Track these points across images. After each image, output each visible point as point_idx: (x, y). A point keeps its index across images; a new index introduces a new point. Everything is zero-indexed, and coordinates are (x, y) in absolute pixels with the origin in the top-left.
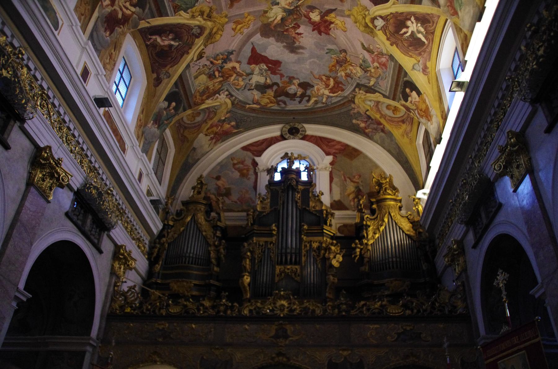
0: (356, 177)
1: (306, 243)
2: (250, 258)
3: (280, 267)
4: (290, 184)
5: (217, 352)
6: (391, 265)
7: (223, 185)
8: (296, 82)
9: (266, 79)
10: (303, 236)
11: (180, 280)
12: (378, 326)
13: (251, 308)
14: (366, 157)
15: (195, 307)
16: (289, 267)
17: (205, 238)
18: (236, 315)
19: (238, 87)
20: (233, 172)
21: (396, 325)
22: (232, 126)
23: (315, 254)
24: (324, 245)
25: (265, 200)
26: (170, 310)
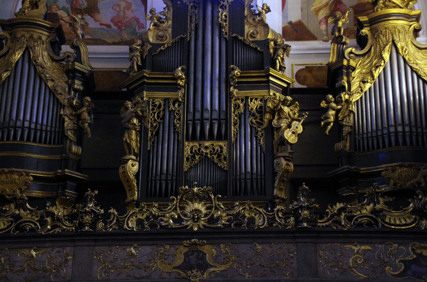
3: (191, 144)
6: (393, 139)
10: (232, 88)
15: (36, 219)
17: (52, 92)
18: (114, 229)
23: (254, 121)
24: (270, 104)
25: (163, 22)
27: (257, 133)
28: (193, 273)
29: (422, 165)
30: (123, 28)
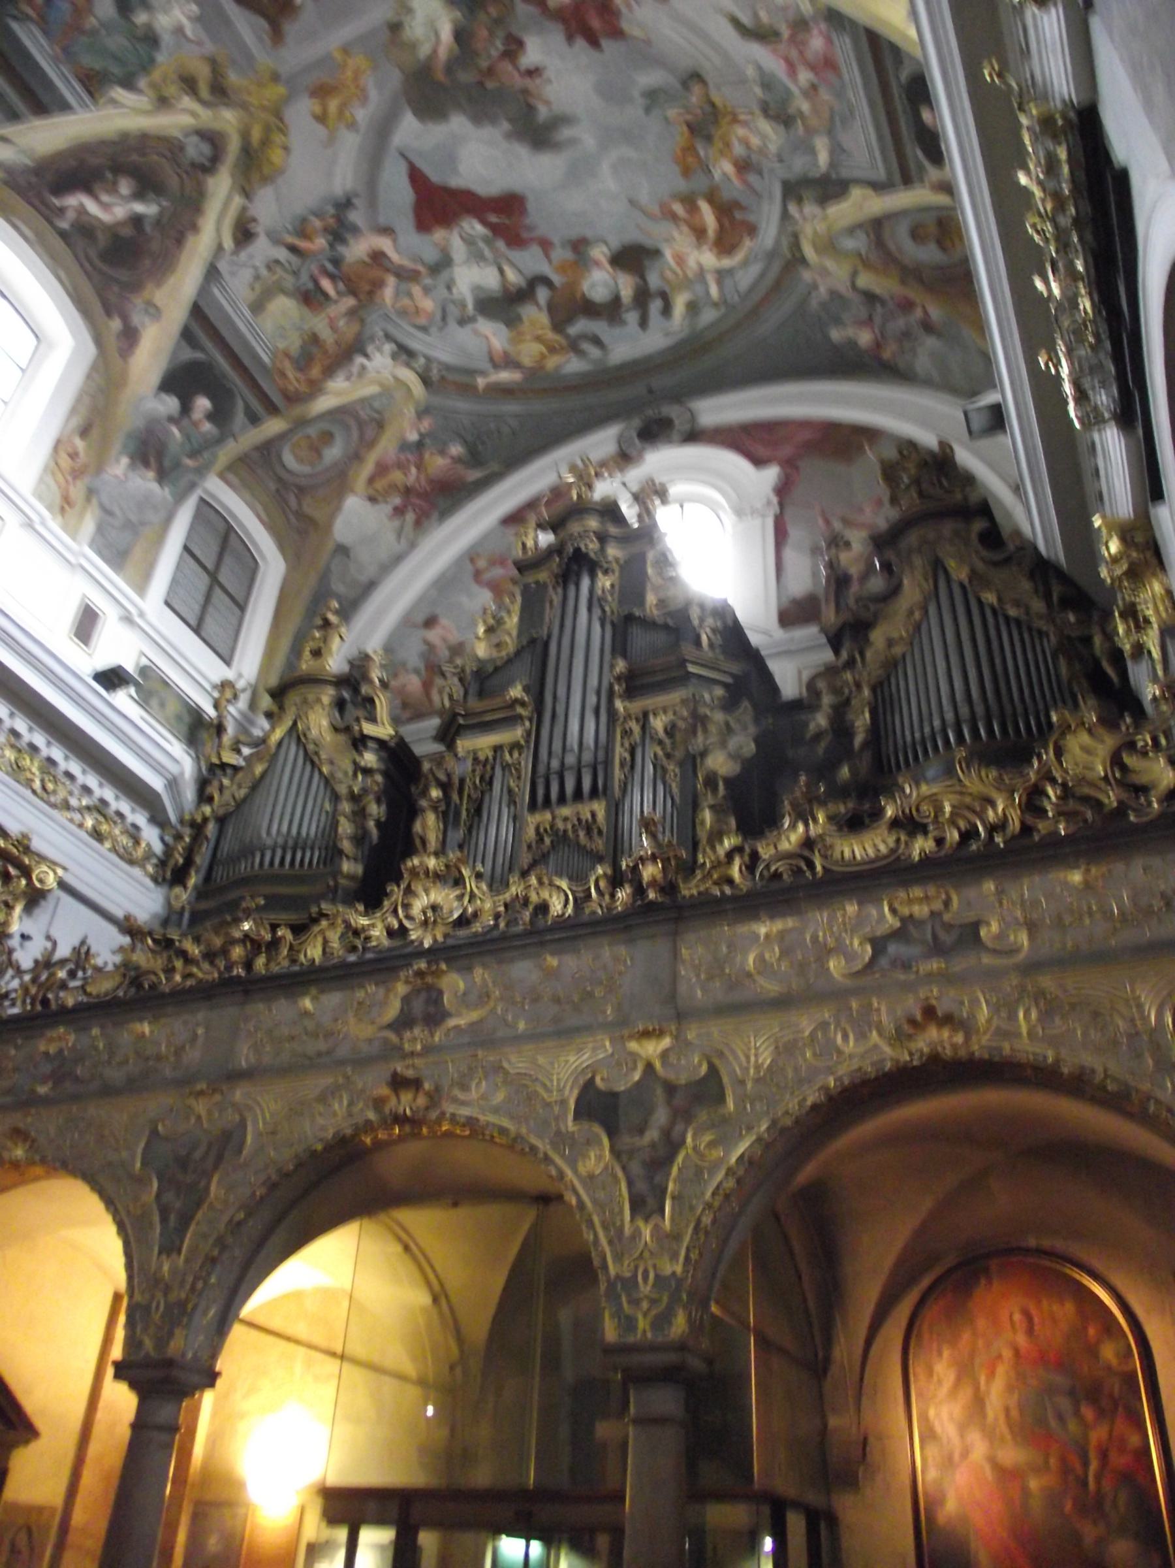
8: (599, 253)
9: (501, 272)
16: (566, 811)
19: (422, 321)
22: (457, 460)
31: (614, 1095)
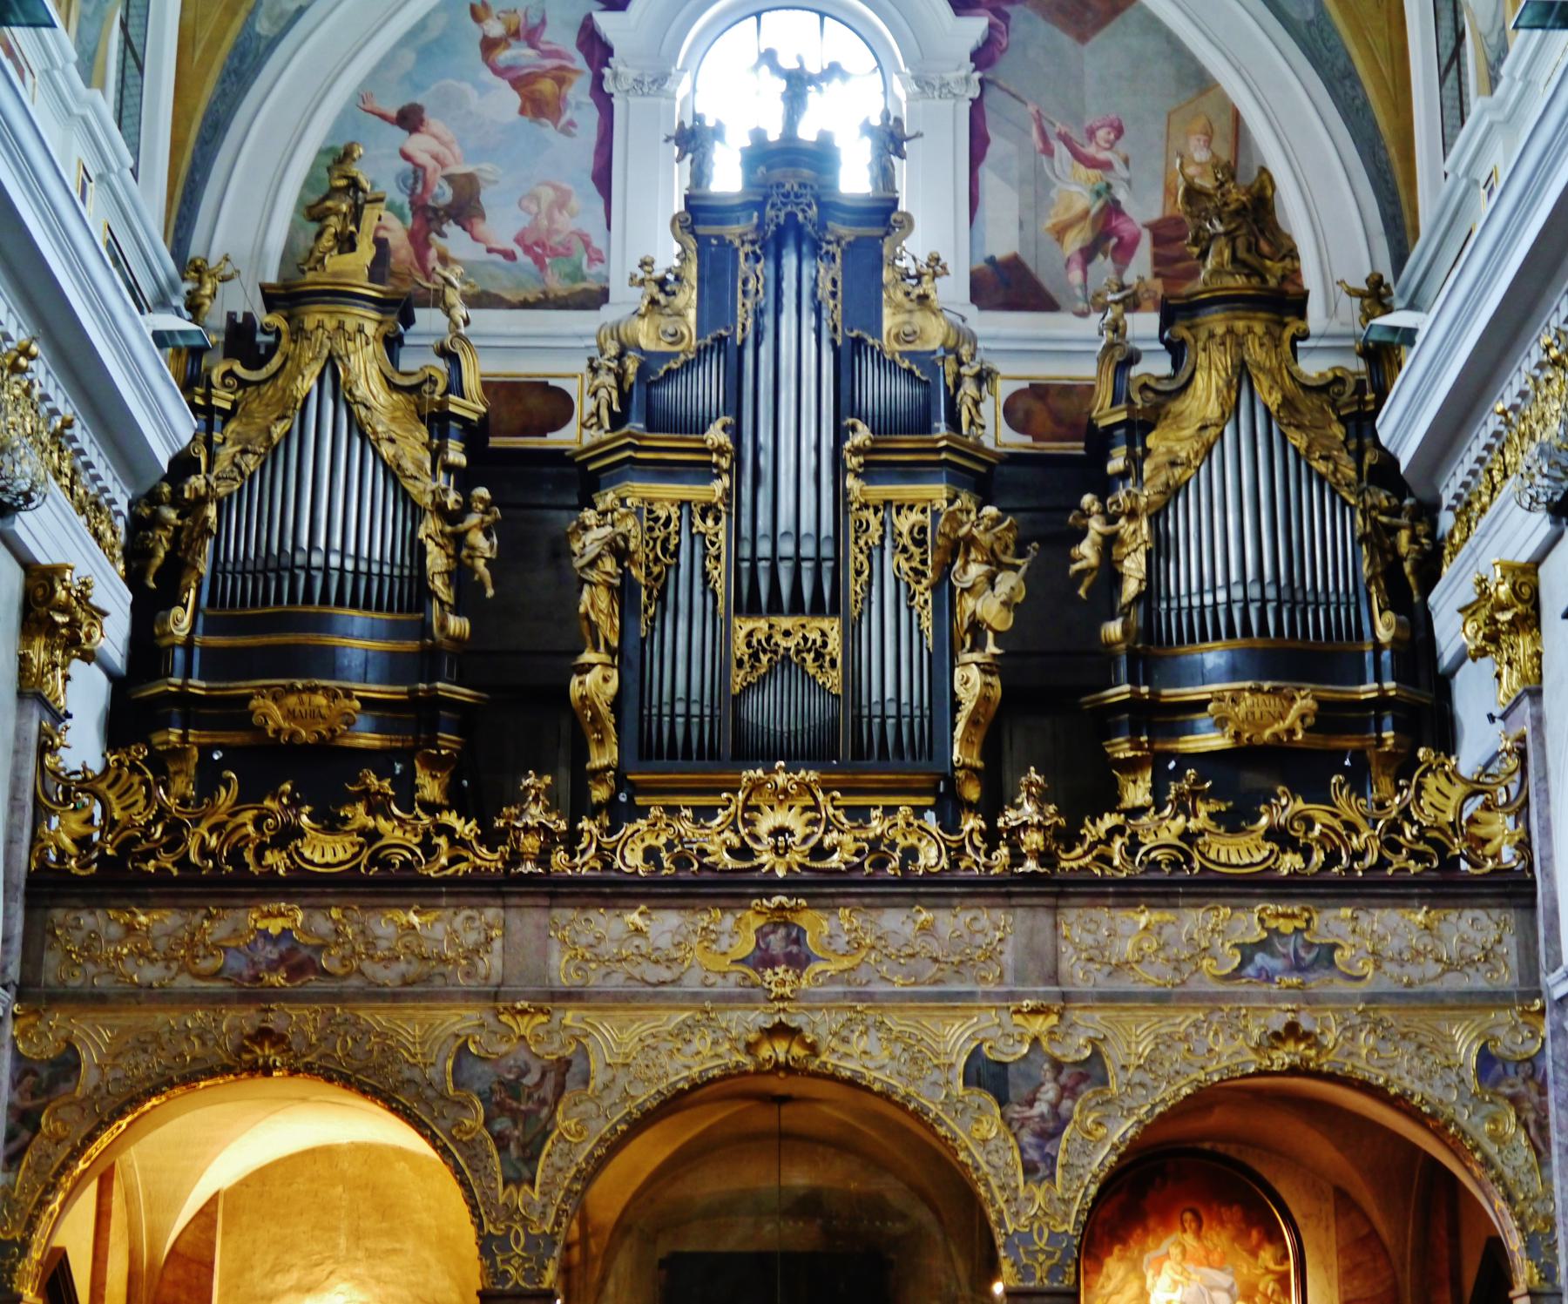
0: (1102, 134)
1: (868, 514)
2: (617, 582)
3: (749, 625)
4: (791, 216)
5: (524, 1026)
7: (436, 158)
10: (851, 482)
11: (299, 684)
12: (1168, 915)
13: (650, 840)
14: (1154, 25)
15: (416, 840)
16: (786, 623)
17: (392, 473)
20: (483, 88)
21: (1239, 914)
26: (307, 854)
27: (912, 598)
28: (776, 974)
29: (1299, 689)
30: (548, 260)
31: (1004, 1065)
